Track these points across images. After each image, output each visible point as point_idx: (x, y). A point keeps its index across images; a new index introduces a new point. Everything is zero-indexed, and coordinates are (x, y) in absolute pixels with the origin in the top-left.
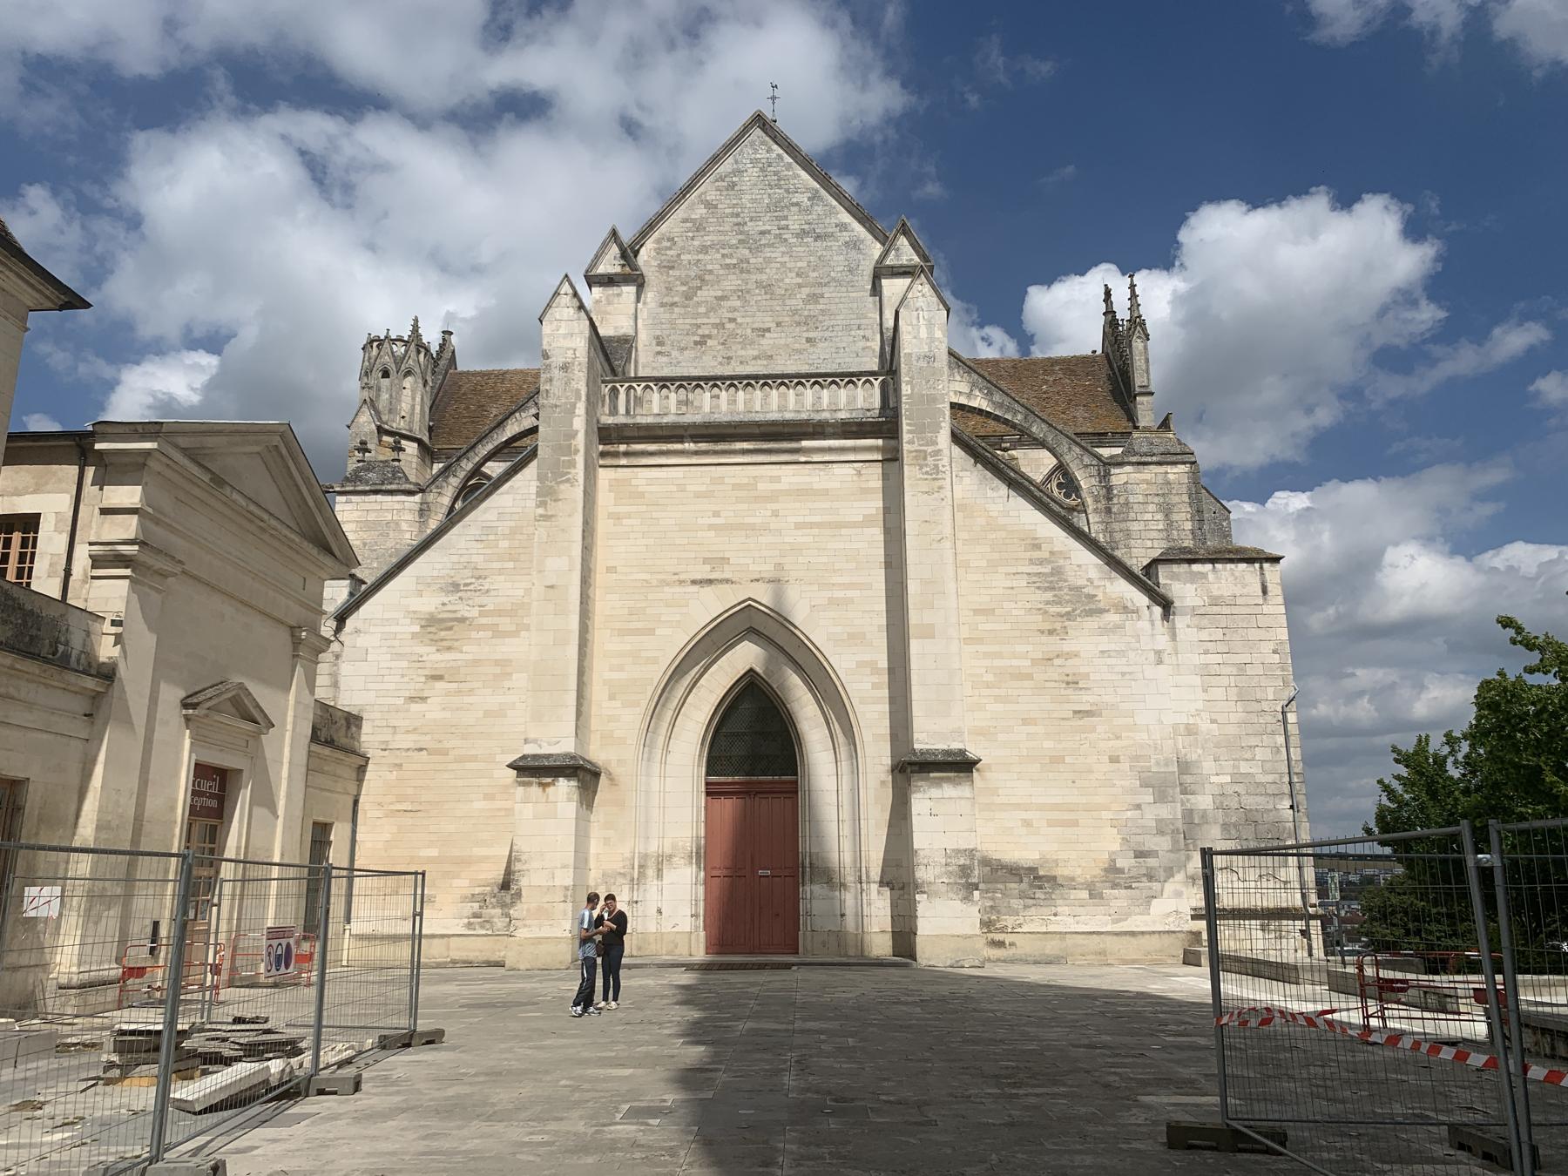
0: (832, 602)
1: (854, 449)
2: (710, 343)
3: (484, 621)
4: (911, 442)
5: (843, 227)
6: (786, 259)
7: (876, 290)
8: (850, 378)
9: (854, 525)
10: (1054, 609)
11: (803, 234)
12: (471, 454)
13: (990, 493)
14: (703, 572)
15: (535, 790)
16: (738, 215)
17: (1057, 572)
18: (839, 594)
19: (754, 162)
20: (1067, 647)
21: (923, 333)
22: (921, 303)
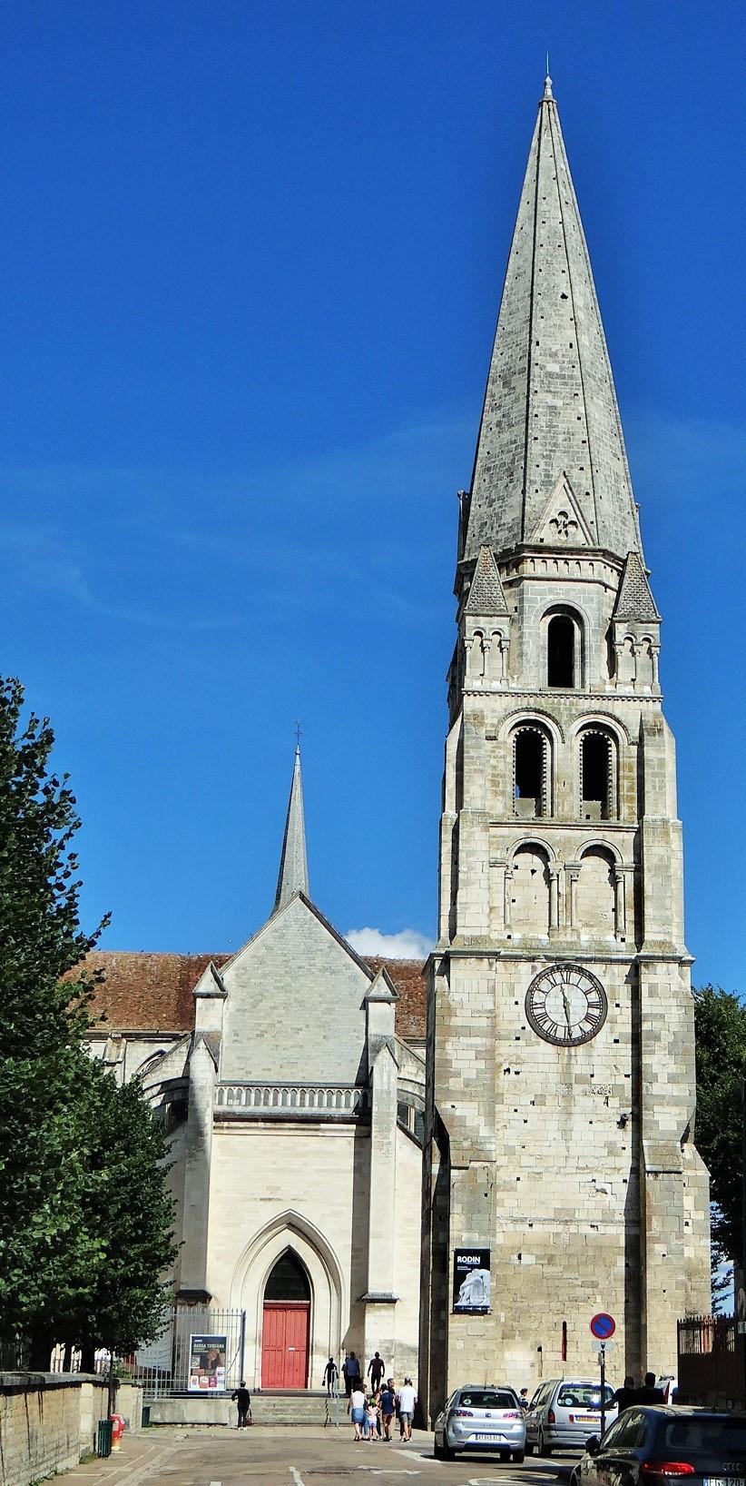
5: (347, 967)
7: (364, 1006)
11: (324, 970)
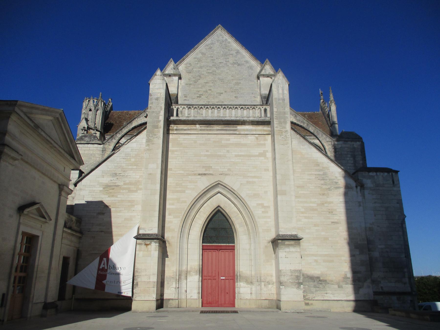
0: (248, 182)
1: (256, 130)
2: (202, 97)
3: (125, 186)
4: (276, 127)
5: (247, 62)
6: (228, 71)
8: (253, 107)
9: (255, 156)
10: (324, 187)
11: (234, 63)
12: (120, 132)
13: (302, 147)
14: (203, 171)
15: (143, 247)
16: (212, 57)
17: (325, 174)
18: (250, 180)
19: (218, 41)
20: (329, 200)
21: (281, 91)
22: (280, 81)
